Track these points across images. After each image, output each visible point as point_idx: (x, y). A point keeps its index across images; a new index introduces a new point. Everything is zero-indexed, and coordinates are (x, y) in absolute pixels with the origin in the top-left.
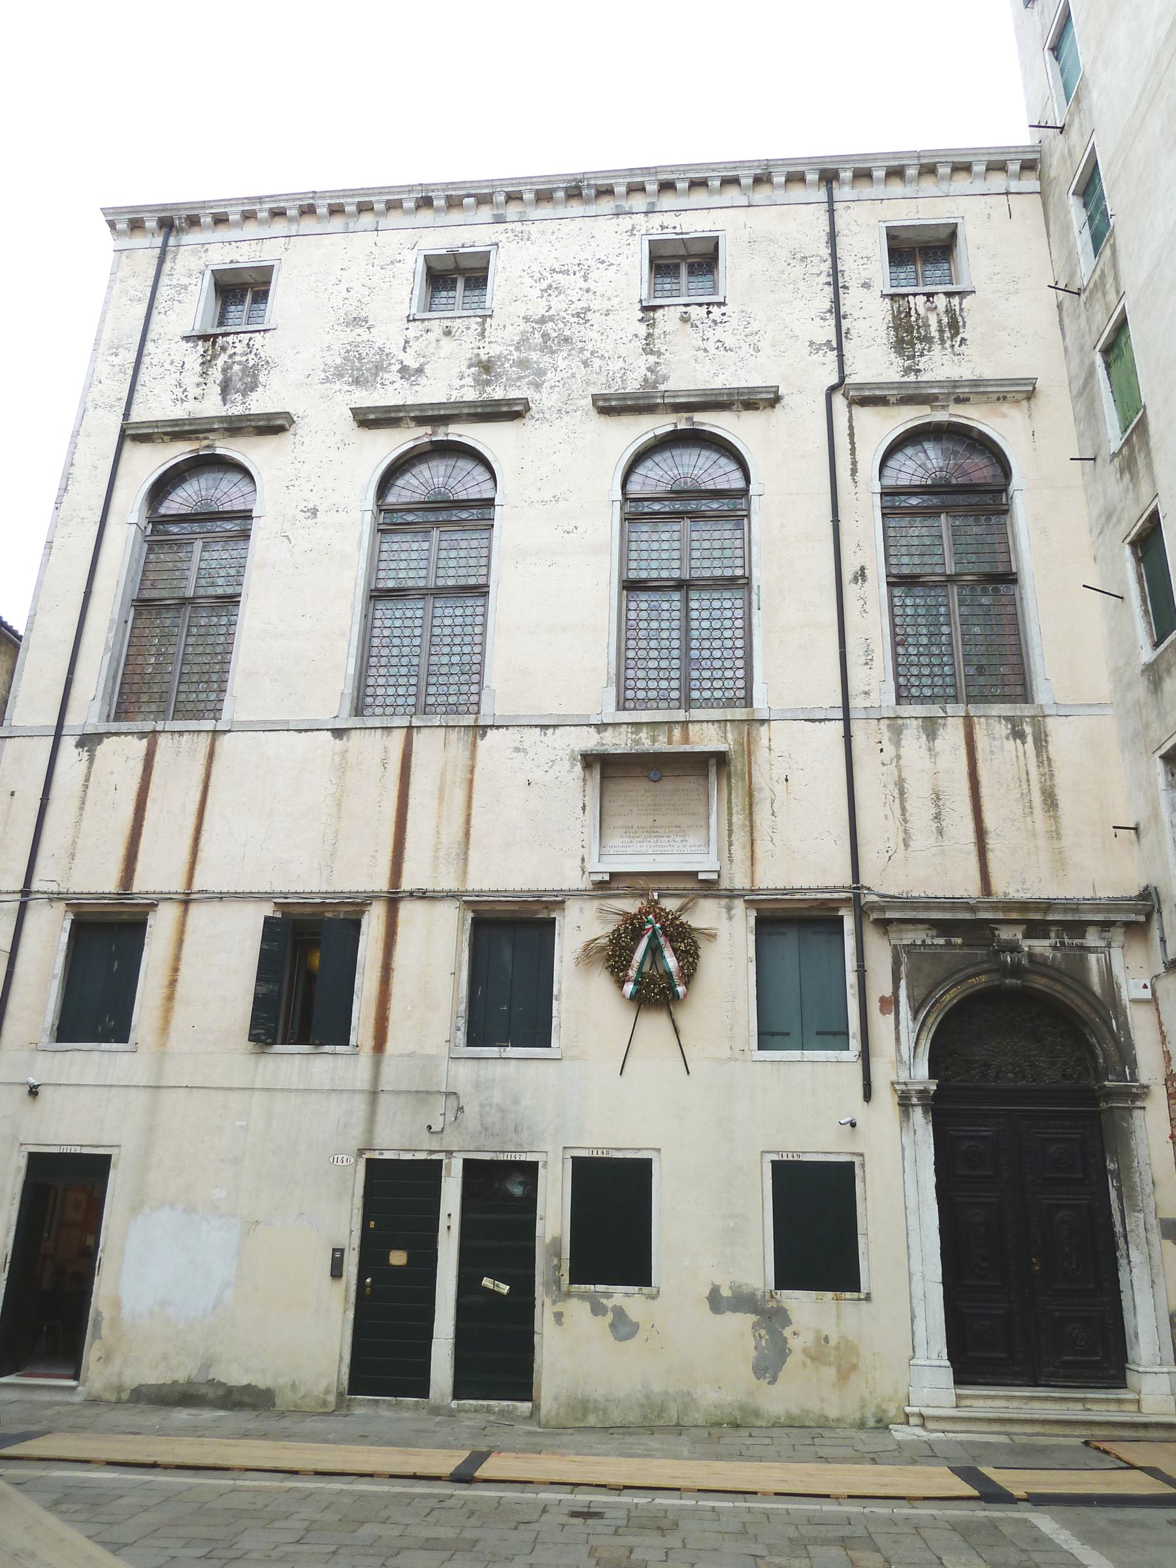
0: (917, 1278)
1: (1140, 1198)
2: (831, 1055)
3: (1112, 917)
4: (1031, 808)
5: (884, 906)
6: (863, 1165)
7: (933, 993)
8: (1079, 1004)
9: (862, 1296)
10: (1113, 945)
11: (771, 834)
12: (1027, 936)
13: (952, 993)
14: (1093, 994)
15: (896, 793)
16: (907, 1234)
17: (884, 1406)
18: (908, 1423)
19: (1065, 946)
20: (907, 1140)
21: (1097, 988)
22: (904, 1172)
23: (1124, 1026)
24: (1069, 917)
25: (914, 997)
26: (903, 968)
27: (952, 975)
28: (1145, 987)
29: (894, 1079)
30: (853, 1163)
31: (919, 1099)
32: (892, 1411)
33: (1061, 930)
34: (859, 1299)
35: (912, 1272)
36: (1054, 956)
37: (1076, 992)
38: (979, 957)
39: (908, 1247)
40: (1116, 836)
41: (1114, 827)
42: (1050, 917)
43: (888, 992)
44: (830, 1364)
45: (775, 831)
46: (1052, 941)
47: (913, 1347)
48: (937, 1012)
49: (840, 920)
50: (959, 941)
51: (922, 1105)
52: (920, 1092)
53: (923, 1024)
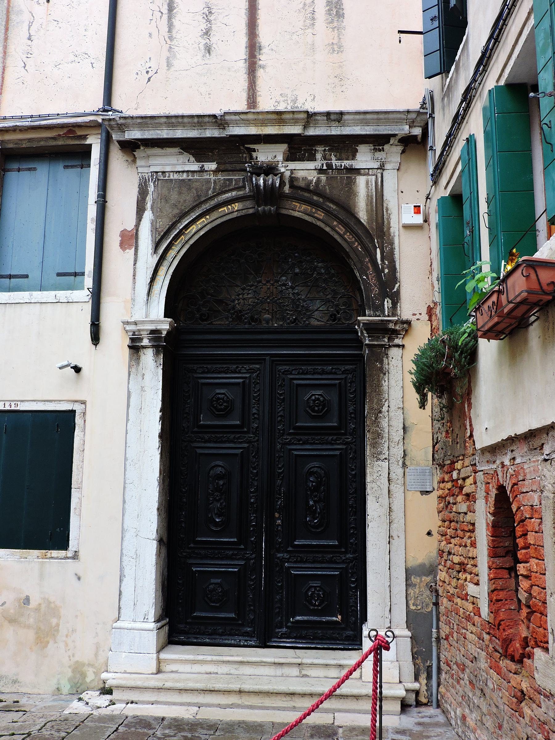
1: (386, 445)
2: (62, 295)
3: (384, 130)
4: (313, 19)
5: (124, 125)
7: (178, 225)
9: (70, 553)
10: (387, 166)
11: (25, 60)
12: (290, 157)
13: (200, 224)
15: (165, 10)
16: (124, 488)
19: (333, 169)
21: (363, 216)
22: (128, 420)
23: (389, 257)
24: (335, 131)
27: (201, 203)
30: (73, 412)
31: (150, 340)
34: (66, 558)
35: (125, 527)
36: (319, 180)
37: (336, 218)
39: (124, 502)
40: (400, 41)
41: (400, 32)
42: (311, 132)
44: (29, 627)
45: (29, 56)
46: (317, 164)
47: (120, 608)
48: (180, 245)
49: (89, 147)
50: (213, 166)
51: (153, 346)
52: (153, 332)
53: (162, 258)
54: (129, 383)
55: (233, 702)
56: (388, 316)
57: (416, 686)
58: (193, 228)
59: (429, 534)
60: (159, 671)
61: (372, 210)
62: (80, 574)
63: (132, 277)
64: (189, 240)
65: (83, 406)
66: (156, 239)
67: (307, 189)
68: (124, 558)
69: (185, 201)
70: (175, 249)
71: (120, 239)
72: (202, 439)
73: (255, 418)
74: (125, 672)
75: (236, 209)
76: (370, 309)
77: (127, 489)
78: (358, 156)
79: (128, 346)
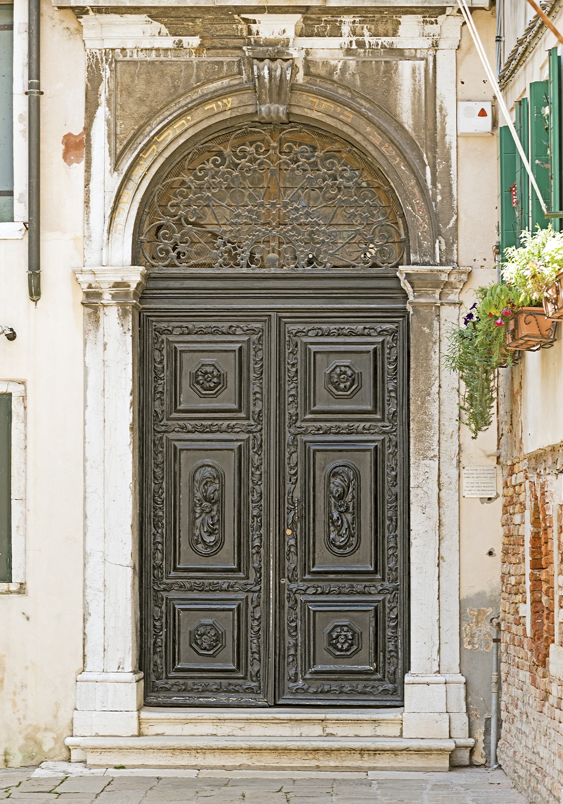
0: (94, 561)
6: (24, 398)
8: (377, 143)
9: (13, 587)
10: (442, 44)
14: (400, 127)
16: (85, 498)
17: (39, 736)
18: (69, 760)
20: (93, 359)
22: (85, 406)
25: (116, 134)
26: (103, 89)
28: (483, 113)
29: (77, 263)
32: (48, 744)
33: (360, 22)
34: (9, 592)
35: (88, 550)
38: (225, 68)
39: (85, 517)
43: (77, 129)
46: (345, 40)
47: (84, 656)
48: (150, 160)
50: (195, 41)
52: (117, 285)
53: (127, 178)
54: (85, 356)
55: (241, 763)
56: (441, 264)
57: (471, 742)
58: (169, 134)
59: (490, 553)
60: (140, 735)
61: (420, 111)
62: (28, 614)
63: (82, 205)
64: (163, 151)
65: (22, 387)
66: (116, 150)
67: (329, 78)
68: (88, 591)
69: (156, 95)
70: (145, 165)
71: (63, 147)
72: (183, 428)
73: (257, 399)
74: (97, 735)
75: (229, 106)
76: (416, 253)
77: (88, 500)
78: (401, 29)
79: (83, 304)
